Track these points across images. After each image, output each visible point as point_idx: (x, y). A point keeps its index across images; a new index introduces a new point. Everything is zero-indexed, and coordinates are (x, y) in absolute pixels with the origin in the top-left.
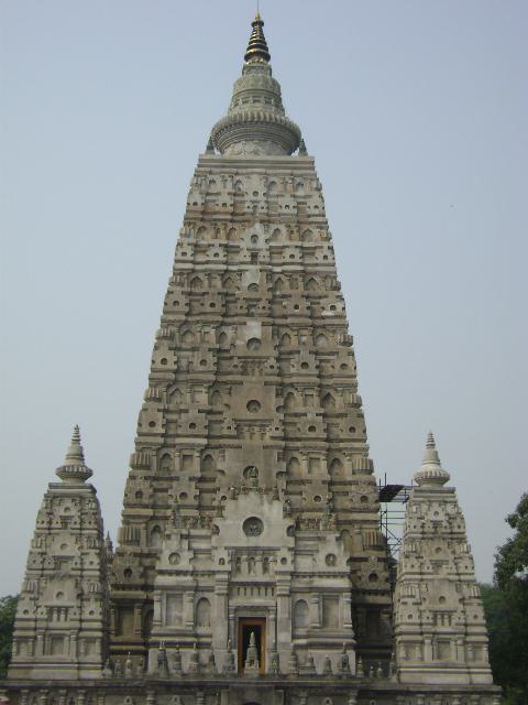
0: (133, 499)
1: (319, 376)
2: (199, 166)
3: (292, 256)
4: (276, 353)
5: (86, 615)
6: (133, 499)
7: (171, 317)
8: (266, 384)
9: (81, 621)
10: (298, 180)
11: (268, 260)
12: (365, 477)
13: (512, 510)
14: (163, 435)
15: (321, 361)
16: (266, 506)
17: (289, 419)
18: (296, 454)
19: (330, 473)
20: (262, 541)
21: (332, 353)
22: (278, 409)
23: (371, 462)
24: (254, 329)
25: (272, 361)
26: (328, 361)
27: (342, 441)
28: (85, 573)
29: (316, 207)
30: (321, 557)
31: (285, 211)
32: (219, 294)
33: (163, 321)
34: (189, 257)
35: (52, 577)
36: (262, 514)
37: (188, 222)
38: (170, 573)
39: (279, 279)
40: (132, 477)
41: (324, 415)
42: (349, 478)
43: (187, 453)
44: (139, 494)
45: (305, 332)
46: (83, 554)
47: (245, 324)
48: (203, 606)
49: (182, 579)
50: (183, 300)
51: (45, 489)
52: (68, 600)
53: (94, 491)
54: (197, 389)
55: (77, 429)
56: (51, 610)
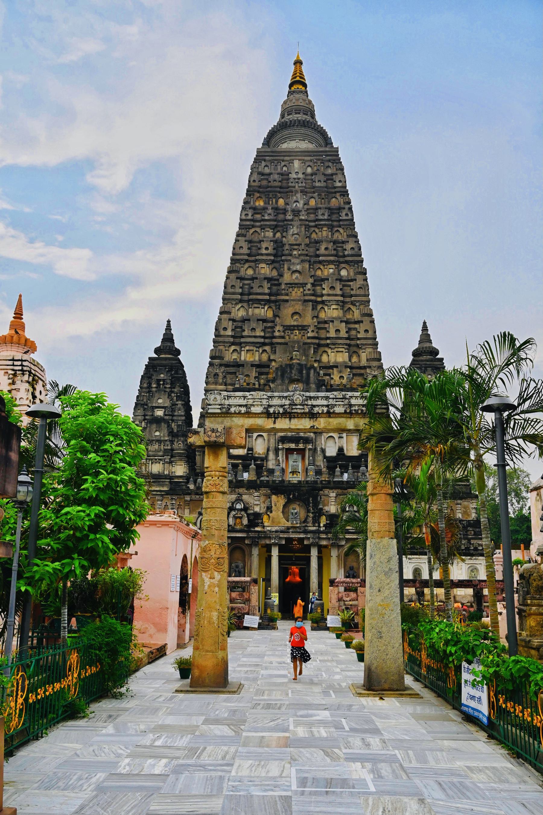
1: (342, 296)
2: (257, 156)
3: (323, 214)
4: (311, 280)
6: (211, 380)
7: (238, 257)
8: (305, 301)
9: (172, 450)
10: (327, 164)
11: (303, 218)
12: (375, 364)
14: (232, 336)
15: (344, 286)
17: (322, 326)
18: (326, 349)
19: (350, 360)
21: (352, 280)
22: (313, 318)
23: (380, 353)
25: (309, 286)
26: (350, 286)
27: (359, 339)
28: (175, 418)
29: (340, 181)
31: (318, 184)
32: (271, 241)
33: (232, 260)
34: (250, 217)
37: (250, 192)
39: (314, 231)
40: (211, 364)
41: (347, 322)
42: (364, 362)
43: (247, 348)
45: (333, 267)
46: (173, 405)
47: (290, 261)
48: (260, 440)
50: (245, 245)
51: (146, 361)
54: (256, 305)
55: (169, 322)
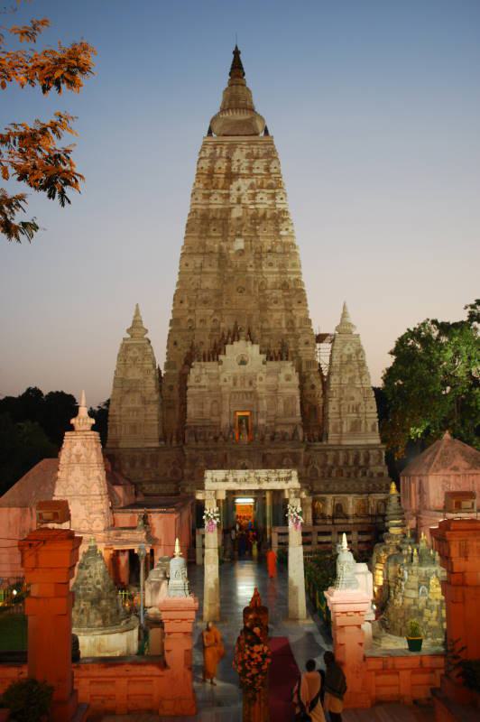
0: (173, 343)
5: (149, 412)
13: (392, 346)
16: (250, 348)
20: (248, 369)
24: (240, 244)
30: (282, 376)
35: (128, 392)
36: (247, 352)
38: (195, 387)
44: (175, 344)
49: (203, 390)
52: (138, 405)
53: (149, 342)
55: (137, 305)
56: (129, 410)
